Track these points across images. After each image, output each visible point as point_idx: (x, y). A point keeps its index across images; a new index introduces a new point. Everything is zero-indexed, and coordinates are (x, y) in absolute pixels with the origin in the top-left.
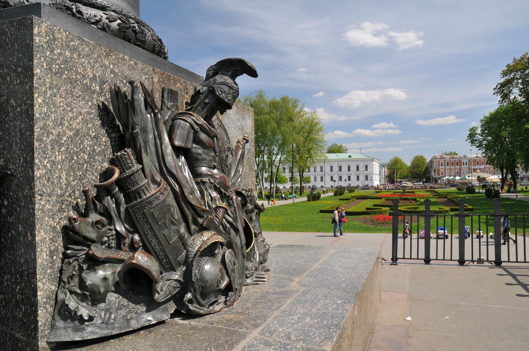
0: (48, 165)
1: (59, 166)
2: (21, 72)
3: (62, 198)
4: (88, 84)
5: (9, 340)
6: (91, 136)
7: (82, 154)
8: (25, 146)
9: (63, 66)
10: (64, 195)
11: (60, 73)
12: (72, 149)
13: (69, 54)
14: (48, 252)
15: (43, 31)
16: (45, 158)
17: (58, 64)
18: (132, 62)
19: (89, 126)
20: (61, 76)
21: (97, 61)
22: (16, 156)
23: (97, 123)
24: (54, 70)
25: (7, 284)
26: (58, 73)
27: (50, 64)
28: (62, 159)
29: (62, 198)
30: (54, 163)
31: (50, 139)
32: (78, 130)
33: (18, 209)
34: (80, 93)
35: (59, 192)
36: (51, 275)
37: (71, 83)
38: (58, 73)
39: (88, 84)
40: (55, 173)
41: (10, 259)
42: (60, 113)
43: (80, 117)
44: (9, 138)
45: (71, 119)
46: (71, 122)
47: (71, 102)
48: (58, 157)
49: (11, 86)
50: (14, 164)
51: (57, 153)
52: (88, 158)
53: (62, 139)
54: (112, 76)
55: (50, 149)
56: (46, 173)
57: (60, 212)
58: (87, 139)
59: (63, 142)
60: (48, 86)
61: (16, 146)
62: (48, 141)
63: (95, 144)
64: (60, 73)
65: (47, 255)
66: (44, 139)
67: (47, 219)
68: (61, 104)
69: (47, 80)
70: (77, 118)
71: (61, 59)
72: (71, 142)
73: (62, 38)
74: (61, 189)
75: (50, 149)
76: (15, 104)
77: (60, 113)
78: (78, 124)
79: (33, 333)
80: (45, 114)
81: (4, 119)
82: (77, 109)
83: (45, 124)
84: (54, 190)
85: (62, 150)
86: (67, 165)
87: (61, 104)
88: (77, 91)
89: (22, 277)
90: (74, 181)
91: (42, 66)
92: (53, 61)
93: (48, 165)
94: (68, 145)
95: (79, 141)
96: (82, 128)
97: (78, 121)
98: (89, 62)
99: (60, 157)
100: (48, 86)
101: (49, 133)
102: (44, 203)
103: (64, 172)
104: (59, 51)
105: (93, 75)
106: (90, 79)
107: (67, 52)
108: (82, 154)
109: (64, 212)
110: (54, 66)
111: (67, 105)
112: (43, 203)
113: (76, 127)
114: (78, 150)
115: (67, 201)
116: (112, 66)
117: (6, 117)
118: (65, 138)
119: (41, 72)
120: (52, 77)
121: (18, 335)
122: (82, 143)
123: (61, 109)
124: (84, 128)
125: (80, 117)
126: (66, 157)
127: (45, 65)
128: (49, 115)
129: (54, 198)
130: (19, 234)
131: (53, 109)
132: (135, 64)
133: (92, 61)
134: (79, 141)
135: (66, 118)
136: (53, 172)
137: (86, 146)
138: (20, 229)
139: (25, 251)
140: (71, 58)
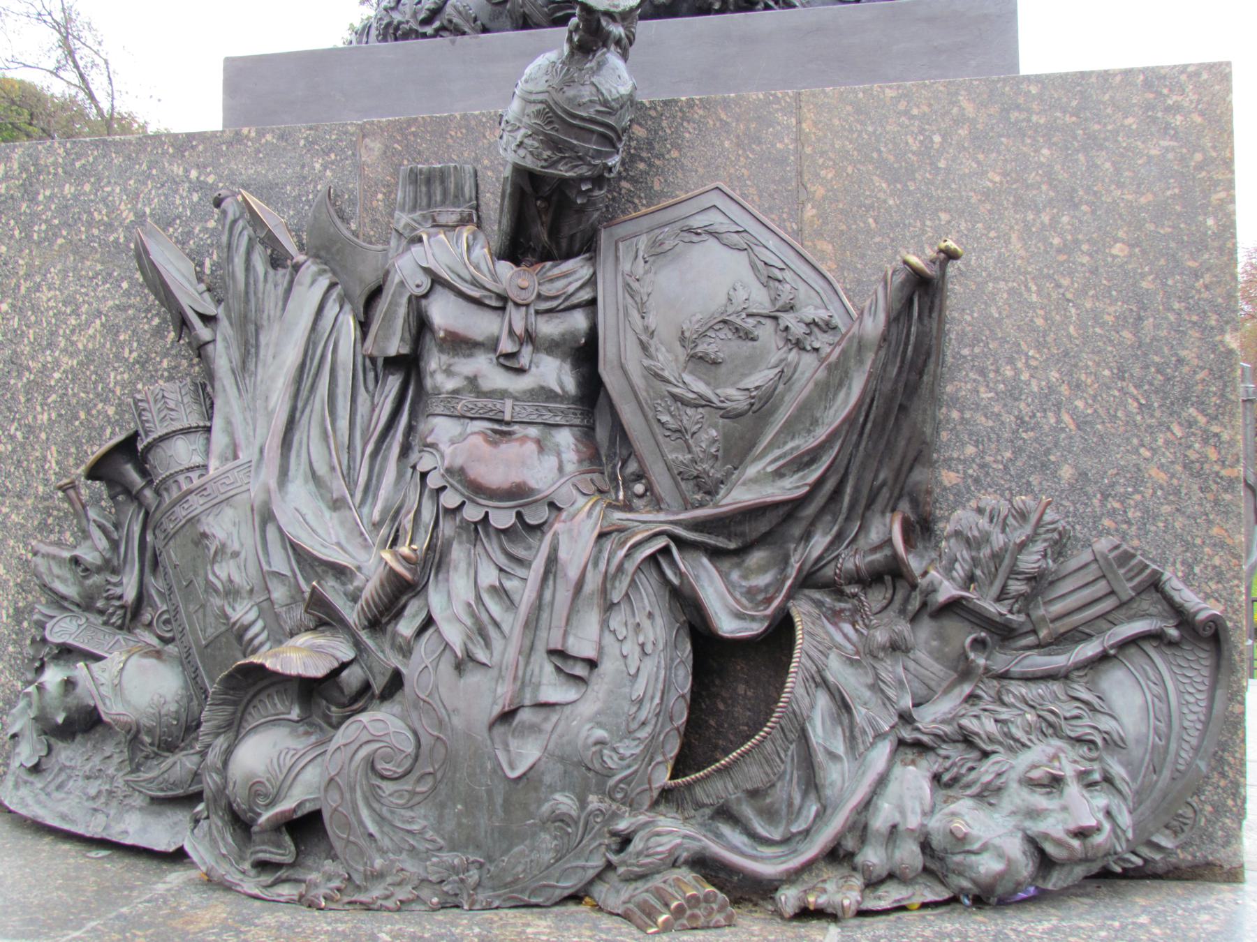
0: (19, 434)
1: (43, 436)
3: (46, 503)
4: (121, 240)
6: (126, 360)
7: (100, 406)
9: (56, 222)
10: (51, 497)
11: (53, 233)
12: (74, 395)
13: (73, 190)
14: (11, 611)
15: (16, 166)
16: (13, 421)
17: (46, 221)
18: (269, 137)
19: (122, 338)
20: (51, 245)
21: (149, 176)
23: (146, 327)
24: (36, 237)
26: (46, 239)
27: (27, 228)
28: (50, 419)
29: (46, 503)
30: (30, 430)
31: (25, 380)
32: (90, 354)
34: (99, 267)
35: (41, 489)
36: (15, 659)
37: (76, 253)
38: (46, 239)
39: (121, 240)
40: (34, 449)
42: (49, 323)
43: (98, 322)
45: (73, 332)
46: (75, 338)
47: (76, 292)
48: (40, 417)
51: (39, 409)
52: (116, 413)
53: (50, 377)
54: (195, 197)
55: (23, 400)
56: (14, 451)
57: (41, 531)
58: (115, 369)
59: (53, 383)
60: (21, 273)
62: (20, 385)
63: (139, 378)
64: (53, 233)
65: (8, 616)
66: (12, 382)
67: (12, 543)
68: (52, 304)
69: (21, 262)
70: (88, 324)
71: (53, 207)
72: (73, 381)
73: (55, 164)
74: (46, 482)
75: (23, 400)
77: (49, 323)
78: (93, 337)
80: (15, 331)
82: (90, 304)
83: (15, 352)
84: (28, 485)
85: (50, 400)
86: (60, 432)
87: (52, 304)
88: (93, 265)
90: (77, 466)
91: (12, 236)
92: (35, 216)
93: (19, 434)
94: (66, 389)
95: (94, 377)
96: (104, 346)
97: (91, 331)
98: (124, 190)
99: (46, 416)
100: (21, 273)
101: (22, 369)
102: (7, 510)
103: (54, 448)
104: (48, 193)
105: (136, 214)
106: (127, 228)
107: (67, 186)
108: (100, 406)
109: (51, 531)
110: (36, 228)
111: (65, 304)
112: (5, 510)
113: (85, 347)
114: (91, 396)
115: (59, 510)
116: (194, 174)
118: (57, 375)
119: (9, 249)
120: (31, 251)
122: (101, 379)
123: (51, 313)
124: (108, 345)
125: (98, 322)
126: (60, 415)
127: (17, 233)
128: (23, 332)
129: (30, 502)
131: (33, 318)
132: (282, 137)
133: (132, 182)
134: (94, 377)
135: (61, 332)
136: (29, 448)
137: (112, 385)
140: (76, 197)
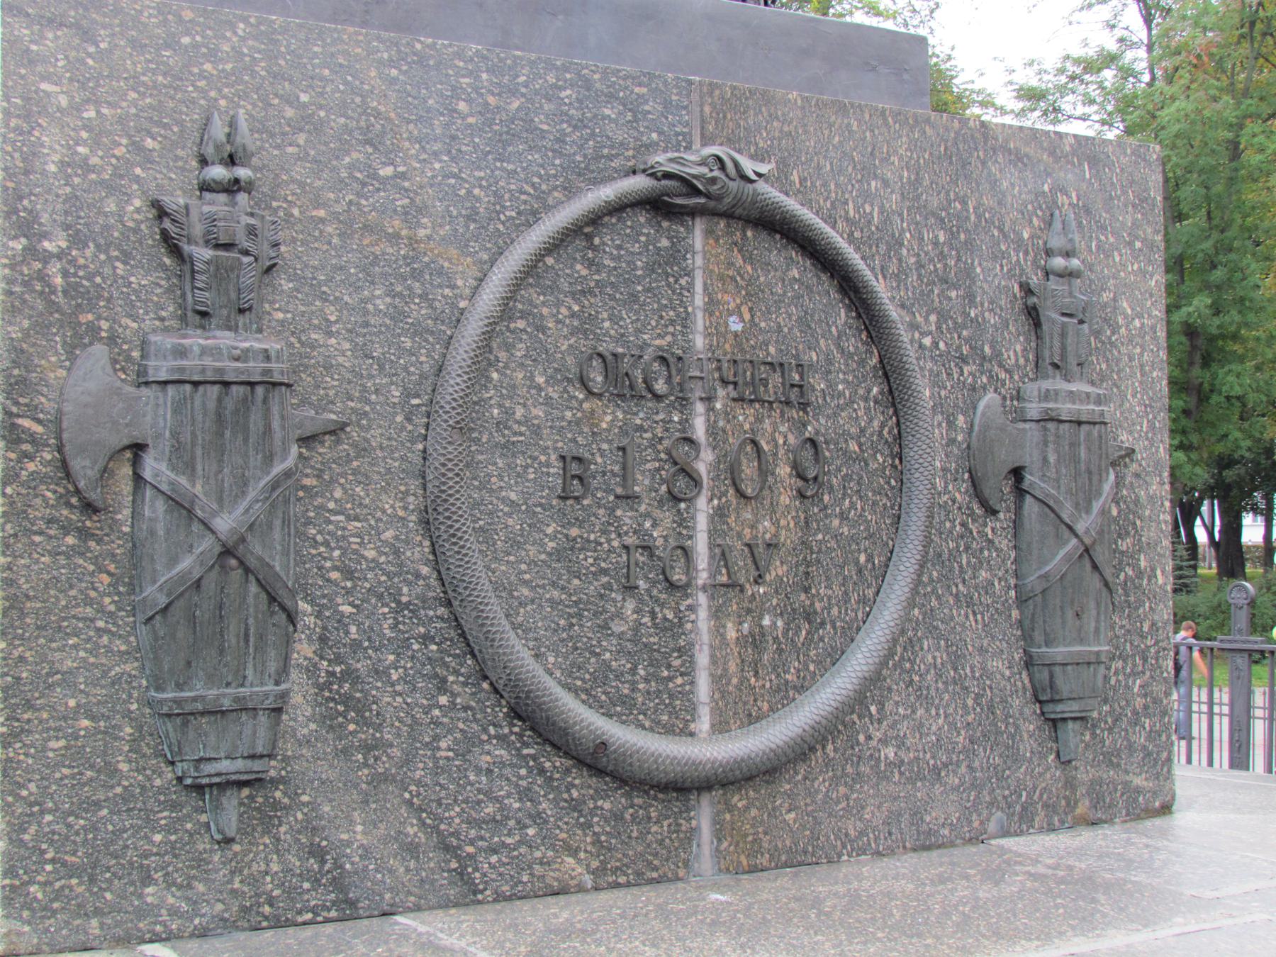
2: (1140, 250)
5: (1122, 795)
8: (1151, 399)
22: (1134, 416)
25: (1118, 681)
33: (1138, 523)
41: (1122, 627)
44: (1120, 378)
49: (1122, 274)
50: (1131, 432)
61: (1134, 396)
76: (1129, 311)
79: (1165, 769)
81: (1110, 338)
89: (1145, 660)
117: (1113, 333)
121: (1138, 781)
130: (1140, 574)
138: (1143, 564)
139: (1150, 608)
